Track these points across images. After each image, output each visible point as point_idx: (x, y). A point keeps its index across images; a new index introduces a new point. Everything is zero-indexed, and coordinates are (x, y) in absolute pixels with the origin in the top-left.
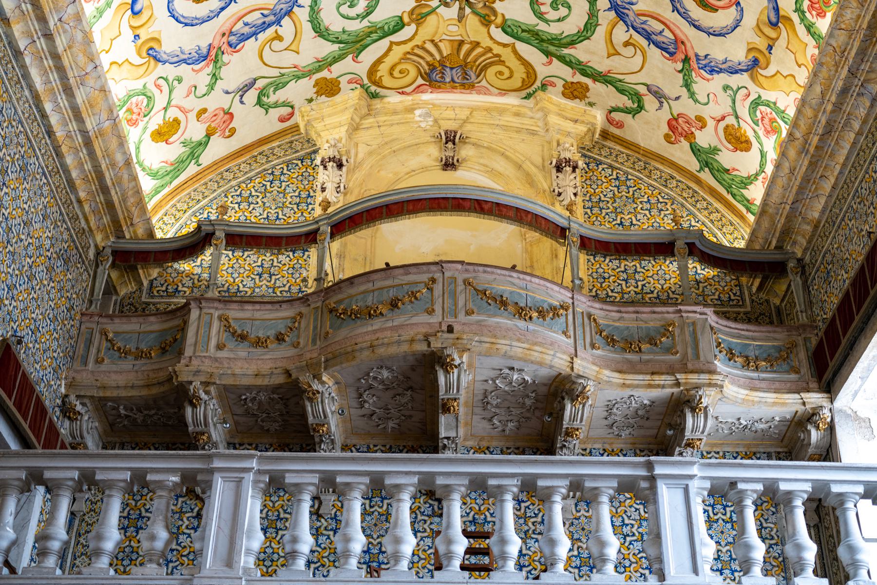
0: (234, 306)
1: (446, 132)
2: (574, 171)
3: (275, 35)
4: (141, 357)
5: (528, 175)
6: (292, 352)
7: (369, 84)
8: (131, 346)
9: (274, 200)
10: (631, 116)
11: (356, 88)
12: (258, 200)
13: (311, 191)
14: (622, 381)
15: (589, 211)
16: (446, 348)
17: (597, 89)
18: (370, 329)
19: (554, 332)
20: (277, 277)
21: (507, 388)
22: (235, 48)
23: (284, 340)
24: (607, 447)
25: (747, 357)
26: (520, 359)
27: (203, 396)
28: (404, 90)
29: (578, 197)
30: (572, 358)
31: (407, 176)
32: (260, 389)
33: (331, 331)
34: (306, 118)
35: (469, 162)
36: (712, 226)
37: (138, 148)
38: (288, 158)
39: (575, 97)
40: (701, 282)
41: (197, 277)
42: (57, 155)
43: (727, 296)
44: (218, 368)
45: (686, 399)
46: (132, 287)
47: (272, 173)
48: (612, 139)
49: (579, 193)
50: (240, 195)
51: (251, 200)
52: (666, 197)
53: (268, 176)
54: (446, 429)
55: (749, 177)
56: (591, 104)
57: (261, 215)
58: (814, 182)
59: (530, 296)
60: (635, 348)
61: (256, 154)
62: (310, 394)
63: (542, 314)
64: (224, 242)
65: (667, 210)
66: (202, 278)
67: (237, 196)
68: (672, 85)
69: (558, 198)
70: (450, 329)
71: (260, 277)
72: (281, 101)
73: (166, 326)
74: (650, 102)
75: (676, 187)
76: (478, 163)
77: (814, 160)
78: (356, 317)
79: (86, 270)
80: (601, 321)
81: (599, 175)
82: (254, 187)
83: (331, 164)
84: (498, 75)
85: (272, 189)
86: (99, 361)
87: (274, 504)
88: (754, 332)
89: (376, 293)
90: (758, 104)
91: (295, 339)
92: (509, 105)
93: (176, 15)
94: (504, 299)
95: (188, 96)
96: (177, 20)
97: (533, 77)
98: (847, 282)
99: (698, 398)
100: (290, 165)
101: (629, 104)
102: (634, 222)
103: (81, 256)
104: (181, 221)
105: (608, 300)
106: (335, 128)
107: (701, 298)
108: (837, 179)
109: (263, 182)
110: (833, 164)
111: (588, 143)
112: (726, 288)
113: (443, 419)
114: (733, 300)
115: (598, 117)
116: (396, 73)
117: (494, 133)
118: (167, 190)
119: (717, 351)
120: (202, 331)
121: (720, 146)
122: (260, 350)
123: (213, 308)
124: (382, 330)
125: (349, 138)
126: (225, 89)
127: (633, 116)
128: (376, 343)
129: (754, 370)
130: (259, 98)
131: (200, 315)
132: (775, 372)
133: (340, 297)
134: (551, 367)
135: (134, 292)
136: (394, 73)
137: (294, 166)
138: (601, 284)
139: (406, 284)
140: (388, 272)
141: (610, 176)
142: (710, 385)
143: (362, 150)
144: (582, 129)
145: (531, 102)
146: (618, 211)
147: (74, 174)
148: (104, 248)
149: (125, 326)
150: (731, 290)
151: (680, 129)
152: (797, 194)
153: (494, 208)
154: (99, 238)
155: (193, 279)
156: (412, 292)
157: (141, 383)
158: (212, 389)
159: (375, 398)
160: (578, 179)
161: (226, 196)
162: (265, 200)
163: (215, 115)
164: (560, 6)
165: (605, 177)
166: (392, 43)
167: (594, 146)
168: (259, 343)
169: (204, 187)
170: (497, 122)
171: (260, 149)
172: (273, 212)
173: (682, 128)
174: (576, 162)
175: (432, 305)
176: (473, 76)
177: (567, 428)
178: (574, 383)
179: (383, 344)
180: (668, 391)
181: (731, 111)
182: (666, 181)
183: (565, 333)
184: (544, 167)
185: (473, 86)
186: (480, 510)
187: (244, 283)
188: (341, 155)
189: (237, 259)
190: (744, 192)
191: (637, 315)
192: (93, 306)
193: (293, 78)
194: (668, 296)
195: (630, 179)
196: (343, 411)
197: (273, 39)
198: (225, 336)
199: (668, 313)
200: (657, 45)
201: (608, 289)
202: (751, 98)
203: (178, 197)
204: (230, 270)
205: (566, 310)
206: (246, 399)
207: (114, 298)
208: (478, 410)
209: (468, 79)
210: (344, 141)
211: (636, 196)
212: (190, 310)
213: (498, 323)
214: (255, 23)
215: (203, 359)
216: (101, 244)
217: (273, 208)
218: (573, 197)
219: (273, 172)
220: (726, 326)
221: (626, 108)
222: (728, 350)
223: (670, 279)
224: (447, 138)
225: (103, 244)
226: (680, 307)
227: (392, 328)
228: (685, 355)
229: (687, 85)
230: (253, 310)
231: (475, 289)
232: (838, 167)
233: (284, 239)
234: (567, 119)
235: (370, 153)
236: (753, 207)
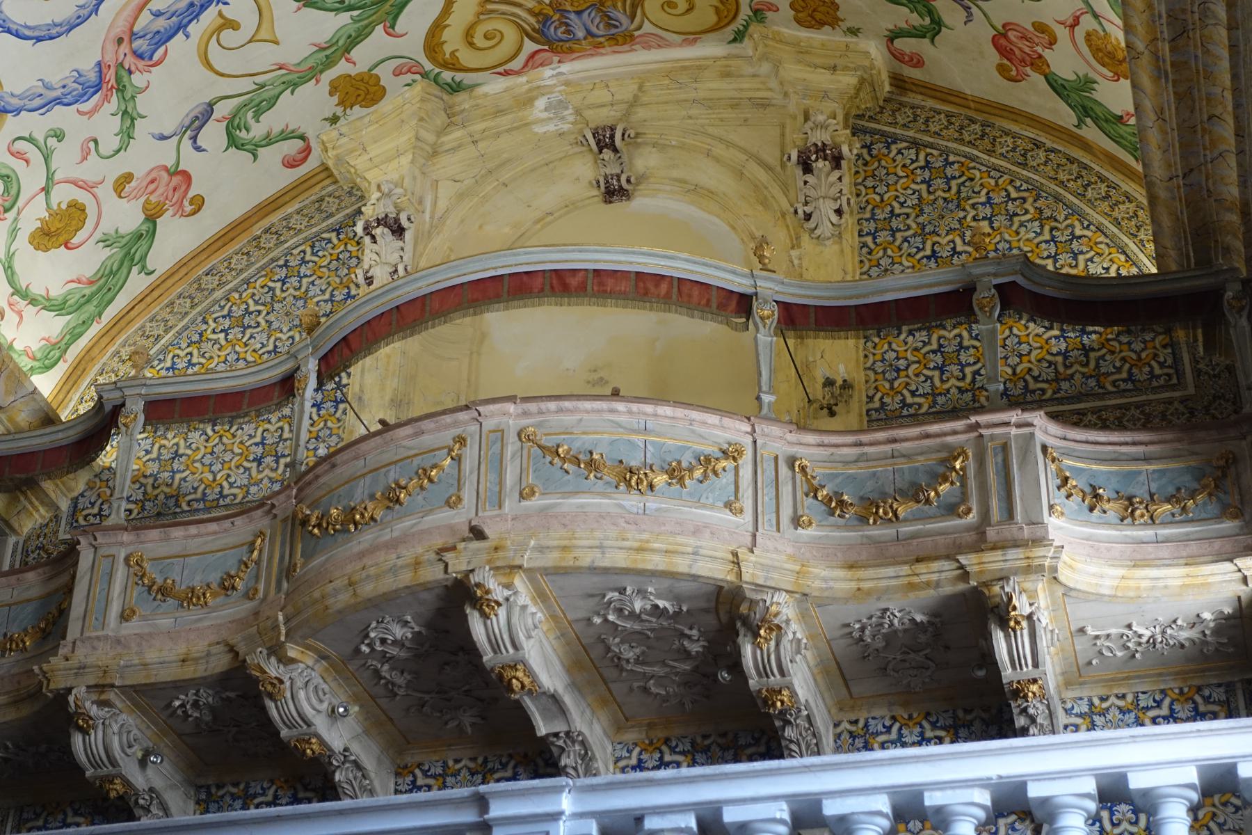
3: (221, 21)
7: (437, 70)
9: (287, 314)
11: (414, 81)
12: (260, 319)
14: (854, 585)
15: (869, 240)
16: (472, 571)
18: (356, 549)
19: (705, 506)
22: (151, 58)
27: (94, 710)
28: (507, 67)
29: (845, 216)
31: (539, 226)
35: (652, 180)
36: (1115, 230)
38: (314, 230)
39: (820, 24)
40: (1093, 349)
41: (150, 481)
47: (285, 265)
48: (914, 88)
49: (845, 207)
50: (229, 315)
52: (1025, 186)
53: (278, 270)
57: (263, 346)
59: (653, 443)
60: (886, 513)
61: (259, 233)
63: (676, 473)
64: (141, 418)
65: (1027, 212)
66: (160, 481)
67: (224, 317)
71: (260, 464)
72: (276, 130)
75: (1046, 164)
76: (670, 179)
78: (335, 531)
81: (890, 165)
82: (254, 294)
84: (666, 7)
85: (284, 295)
89: (368, 478)
91: (252, 583)
92: (705, 59)
93: (14, 27)
94: (595, 456)
95: (84, 159)
96: (18, 35)
100: (317, 244)
105: (905, 412)
106: (389, 160)
107: (1092, 382)
109: (271, 284)
111: (866, 102)
114: (1159, 377)
115: (874, 50)
116: (479, 41)
117: (690, 117)
119: (1059, 497)
122: (193, 614)
123: (115, 544)
124: (373, 549)
125: (423, 173)
126: (157, 132)
127: (932, 41)
128: (356, 578)
129: (1146, 524)
130: (229, 134)
132: (1192, 521)
134: (695, 578)
135: (47, 525)
136: (475, 41)
137: (323, 244)
138: (891, 382)
140: (388, 435)
141: (913, 162)
142: (1028, 570)
143: (446, 192)
144: (848, 80)
145: (747, 47)
146: (927, 230)
150: (1155, 356)
153: (590, 282)
156: (425, 470)
160: (846, 180)
161: (205, 322)
162: (271, 317)
163: (152, 181)
165: (904, 166)
167: (882, 108)
168: (191, 598)
170: (693, 95)
171: (265, 223)
172: (284, 337)
173: (1020, 49)
174: (837, 146)
175: (459, 490)
176: (625, 21)
182: (1024, 155)
187: (232, 480)
189: (221, 437)
191: (894, 446)
193: (283, 87)
194: (1026, 387)
195: (953, 163)
197: (220, 29)
199: (955, 433)
201: (905, 392)
204: (207, 460)
206: (182, 706)
207: (12, 540)
209: (616, 27)
210: (407, 183)
211: (963, 195)
213: (582, 506)
214: (173, 9)
215: (96, 643)
217: (285, 330)
218: (834, 218)
219: (287, 261)
220: (1087, 442)
221: (914, 27)
222: (1088, 490)
223: (1029, 353)
224: (598, 143)
226: (973, 419)
227: (393, 545)
230: (186, 537)
231: (539, 446)
234: (816, 66)
235: (461, 196)
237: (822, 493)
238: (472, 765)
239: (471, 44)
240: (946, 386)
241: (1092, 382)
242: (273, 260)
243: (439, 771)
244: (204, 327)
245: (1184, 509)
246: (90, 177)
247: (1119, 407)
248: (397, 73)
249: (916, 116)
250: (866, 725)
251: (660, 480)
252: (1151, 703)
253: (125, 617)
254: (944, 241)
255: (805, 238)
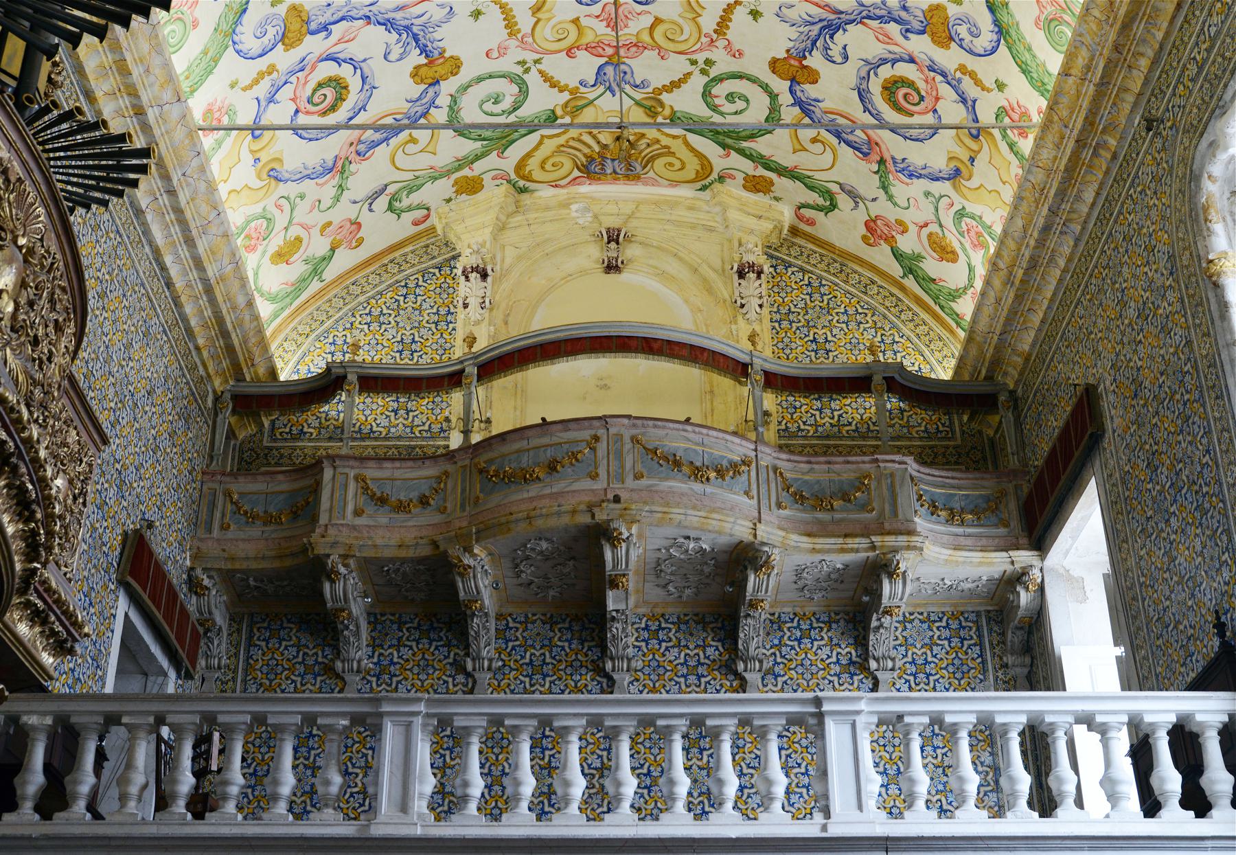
0: (371, 464)
1: (608, 231)
2: (759, 277)
3: (409, 138)
4: (271, 522)
5: (705, 280)
6: (438, 518)
8: (259, 509)
10: (823, 213)
12: (391, 319)
13: (451, 306)
15: (776, 325)
17: (782, 184)
18: (525, 495)
19: (734, 494)
20: (415, 413)
21: (682, 557)
23: (428, 504)
24: (798, 610)
25: (951, 510)
26: (696, 529)
27: (342, 570)
30: (755, 524)
32: (403, 561)
33: (481, 495)
34: (444, 221)
37: (256, 274)
39: (759, 191)
41: (324, 415)
42: (176, 305)
43: (935, 426)
44: (357, 538)
45: (883, 562)
46: (252, 429)
47: (406, 286)
49: (765, 304)
50: (370, 314)
51: (382, 319)
53: (401, 288)
54: (614, 602)
55: (957, 290)
56: (777, 199)
57: (394, 337)
58: (1022, 314)
59: (707, 453)
62: (461, 569)
63: (720, 473)
64: (357, 387)
65: (867, 322)
68: (867, 183)
69: (741, 310)
70: (617, 499)
71: (396, 414)
72: (415, 203)
73: (296, 485)
74: (843, 201)
76: (648, 265)
77: (1019, 293)
78: (510, 481)
79: (206, 422)
80: (788, 475)
81: (788, 280)
83: (474, 274)
86: (224, 527)
87: (423, 683)
88: (959, 479)
89: (531, 453)
90: (963, 216)
97: (709, 169)
98: (1056, 430)
99: (895, 562)
101: (820, 201)
102: (830, 338)
103: (200, 408)
104: (304, 348)
105: (800, 434)
106: (477, 230)
107: (905, 430)
108: (1045, 313)
109: (397, 297)
110: (1041, 298)
111: (774, 240)
112: (933, 418)
113: (610, 594)
114: (942, 432)
115: (786, 214)
116: (548, 166)
118: (287, 312)
119: (918, 508)
120: (337, 495)
121: (924, 254)
122: (402, 516)
123: (348, 466)
127: (826, 214)
128: (533, 514)
130: (390, 203)
131: (334, 476)
132: (982, 526)
133: (490, 455)
134: (731, 535)
135: (255, 435)
138: (792, 414)
139: (565, 443)
142: (908, 548)
143: (510, 253)
144: (767, 226)
147: (193, 323)
148: (222, 392)
149: (250, 485)
151: (879, 231)
152: (1004, 325)
154: (217, 383)
155: (320, 418)
156: (573, 453)
157: (273, 553)
158: (351, 562)
159: (533, 568)
160: (764, 286)
161: (353, 315)
162: (398, 319)
164: (736, 99)
166: (542, 136)
168: (401, 507)
169: (328, 304)
170: (668, 217)
171: (391, 257)
172: (408, 334)
174: (761, 266)
175: (596, 468)
176: (639, 168)
177: (751, 600)
178: (758, 551)
179: (541, 515)
180: (863, 555)
181: (933, 218)
182: (865, 287)
183: (747, 493)
184: (723, 271)
185: (639, 178)
186: (654, 687)
187: (378, 422)
188: (485, 263)
190: (952, 304)
192: (214, 463)
194: (869, 428)
196: (497, 585)
197: (406, 143)
198: (362, 500)
199: (864, 462)
200: (848, 143)
202: (955, 208)
203: (299, 318)
205: (749, 466)
206: (388, 571)
207: (232, 443)
208: (652, 578)
210: (488, 245)
212: (322, 469)
213: (670, 487)
215: (341, 528)
216: (219, 389)
217: (408, 328)
218: (758, 309)
220: (929, 475)
225: (222, 389)
227: (552, 496)
228: (882, 513)
229: (885, 187)
232: (1046, 302)
233: (425, 381)
235: (519, 258)
236: (963, 323)
237: (792, 490)
238: (543, 618)
239: (543, 168)
240: (823, 421)
241: (905, 430)
242: (397, 282)
243: (523, 619)
244: (353, 319)
245: (979, 518)
246: (310, 223)
247: (920, 446)
248: (494, 178)
249: (802, 252)
250: (779, 617)
251: (713, 475)
252: (937, 619)
253: (358, 513)
254: (820, 332)
255: (740, 318)
